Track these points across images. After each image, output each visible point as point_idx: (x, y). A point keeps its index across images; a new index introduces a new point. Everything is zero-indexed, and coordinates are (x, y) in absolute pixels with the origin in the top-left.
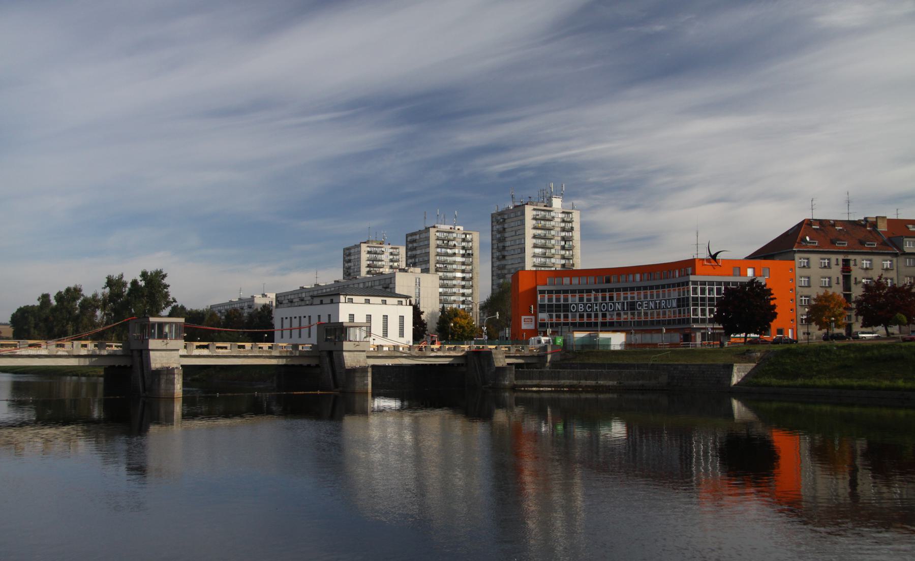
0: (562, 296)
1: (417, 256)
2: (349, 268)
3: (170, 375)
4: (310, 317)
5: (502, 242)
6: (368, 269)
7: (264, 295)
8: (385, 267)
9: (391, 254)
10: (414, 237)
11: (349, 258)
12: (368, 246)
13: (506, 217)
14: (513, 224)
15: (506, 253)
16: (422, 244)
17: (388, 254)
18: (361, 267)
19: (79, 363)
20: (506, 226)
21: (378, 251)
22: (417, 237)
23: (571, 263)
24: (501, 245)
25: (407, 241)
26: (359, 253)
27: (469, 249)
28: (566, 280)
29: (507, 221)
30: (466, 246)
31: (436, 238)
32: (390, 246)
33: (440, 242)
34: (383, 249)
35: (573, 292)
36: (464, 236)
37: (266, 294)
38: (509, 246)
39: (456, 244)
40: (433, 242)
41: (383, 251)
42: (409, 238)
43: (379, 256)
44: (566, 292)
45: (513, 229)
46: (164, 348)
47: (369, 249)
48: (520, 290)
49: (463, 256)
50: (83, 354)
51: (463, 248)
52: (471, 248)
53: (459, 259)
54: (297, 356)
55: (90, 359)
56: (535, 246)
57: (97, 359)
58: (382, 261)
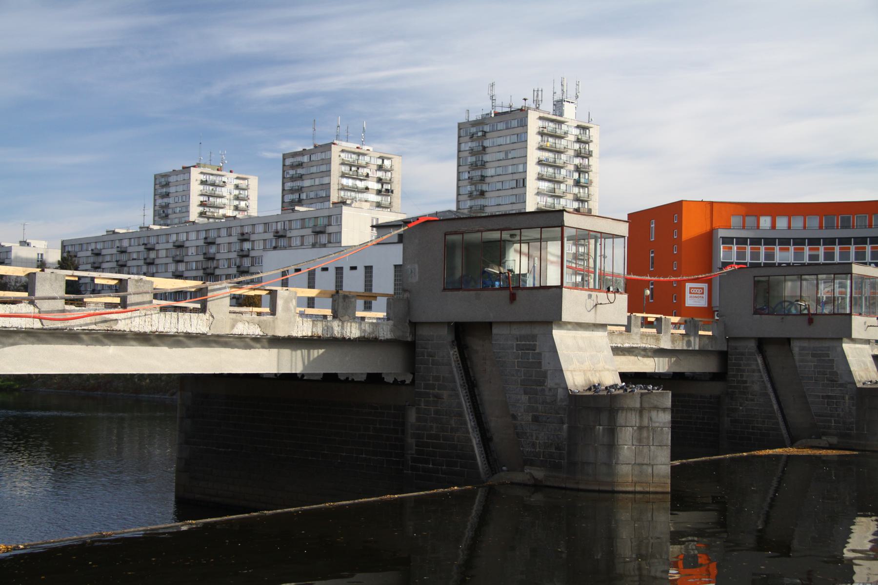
0: (763, 249)
1: (303, 189)
2: (167, 206)
3: (654, 414)
4: (369, 269)
5: (480, 168)
6: (201, 209)
7: (24, 243)
8: (227, 207)
9: (237, 187)
10: (299, 159)
11: (164, 190)
12: (202, 173)
13: (487, 128)
14: (501, 141)
15: (485, 187)
16: (314, 170)
17: (232, 187)
18: (191, 205)
19: (278, 370)
20: (487, 143)
21: (217, 182)
22: (305, 159)
23: (586, 207)
24: (477, 174)
25: (284, 165)
26: (187, 182)
27: (386, 183)
28: (765, 222)
29: (488, 135)
30: (383, 178)
31: (341, 161)
32: (234, 175)
33: (345, 169)
34: (224, 179)
35: (784, 242)
36: (380, 162)
37: (28, 241)
38: (492, 176)
39: (370, 173)
40: (336, 168)
41: (224, 182)
42: (288, 162)
43: (218, 189)
44: (770, 242)
45: (501, 149)
46: (589, 318)
47: (203, 177)
48: (683, 240)
49: (379, 192)
50: (300, 335)
51: (380, 180)
52: (390, 182)
53: (373, 198)
54: (697, 350)
55: (305, 352)
56: (541, 178)
57: (321, 351)
58: (222, 197)
